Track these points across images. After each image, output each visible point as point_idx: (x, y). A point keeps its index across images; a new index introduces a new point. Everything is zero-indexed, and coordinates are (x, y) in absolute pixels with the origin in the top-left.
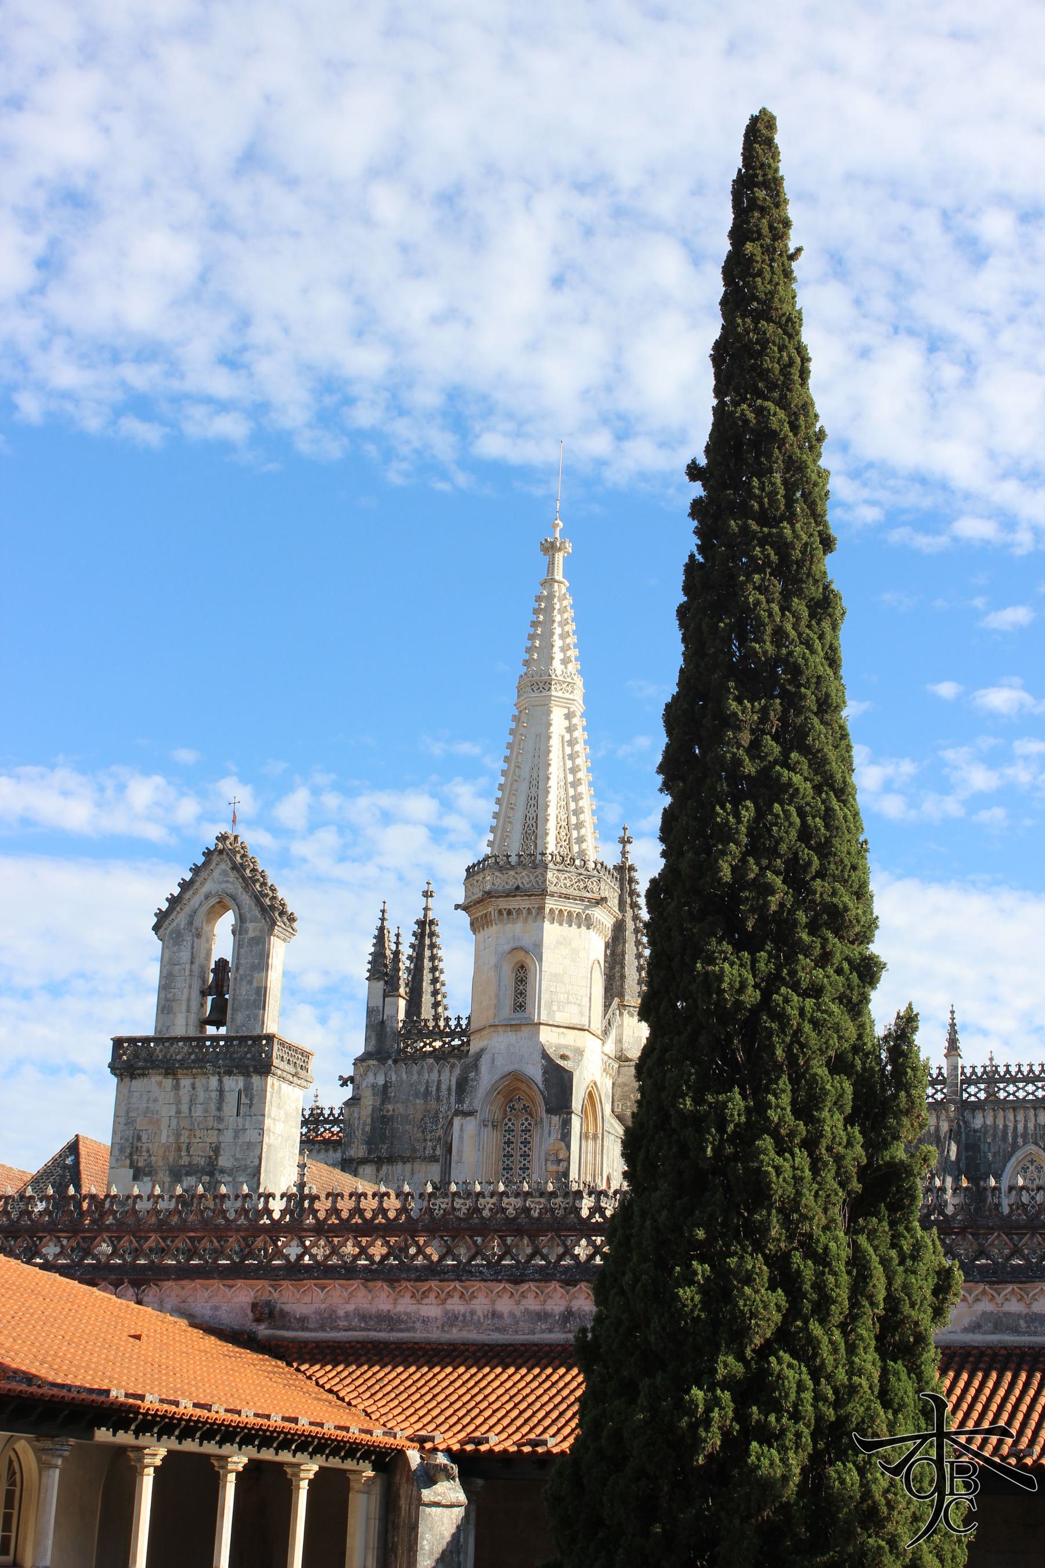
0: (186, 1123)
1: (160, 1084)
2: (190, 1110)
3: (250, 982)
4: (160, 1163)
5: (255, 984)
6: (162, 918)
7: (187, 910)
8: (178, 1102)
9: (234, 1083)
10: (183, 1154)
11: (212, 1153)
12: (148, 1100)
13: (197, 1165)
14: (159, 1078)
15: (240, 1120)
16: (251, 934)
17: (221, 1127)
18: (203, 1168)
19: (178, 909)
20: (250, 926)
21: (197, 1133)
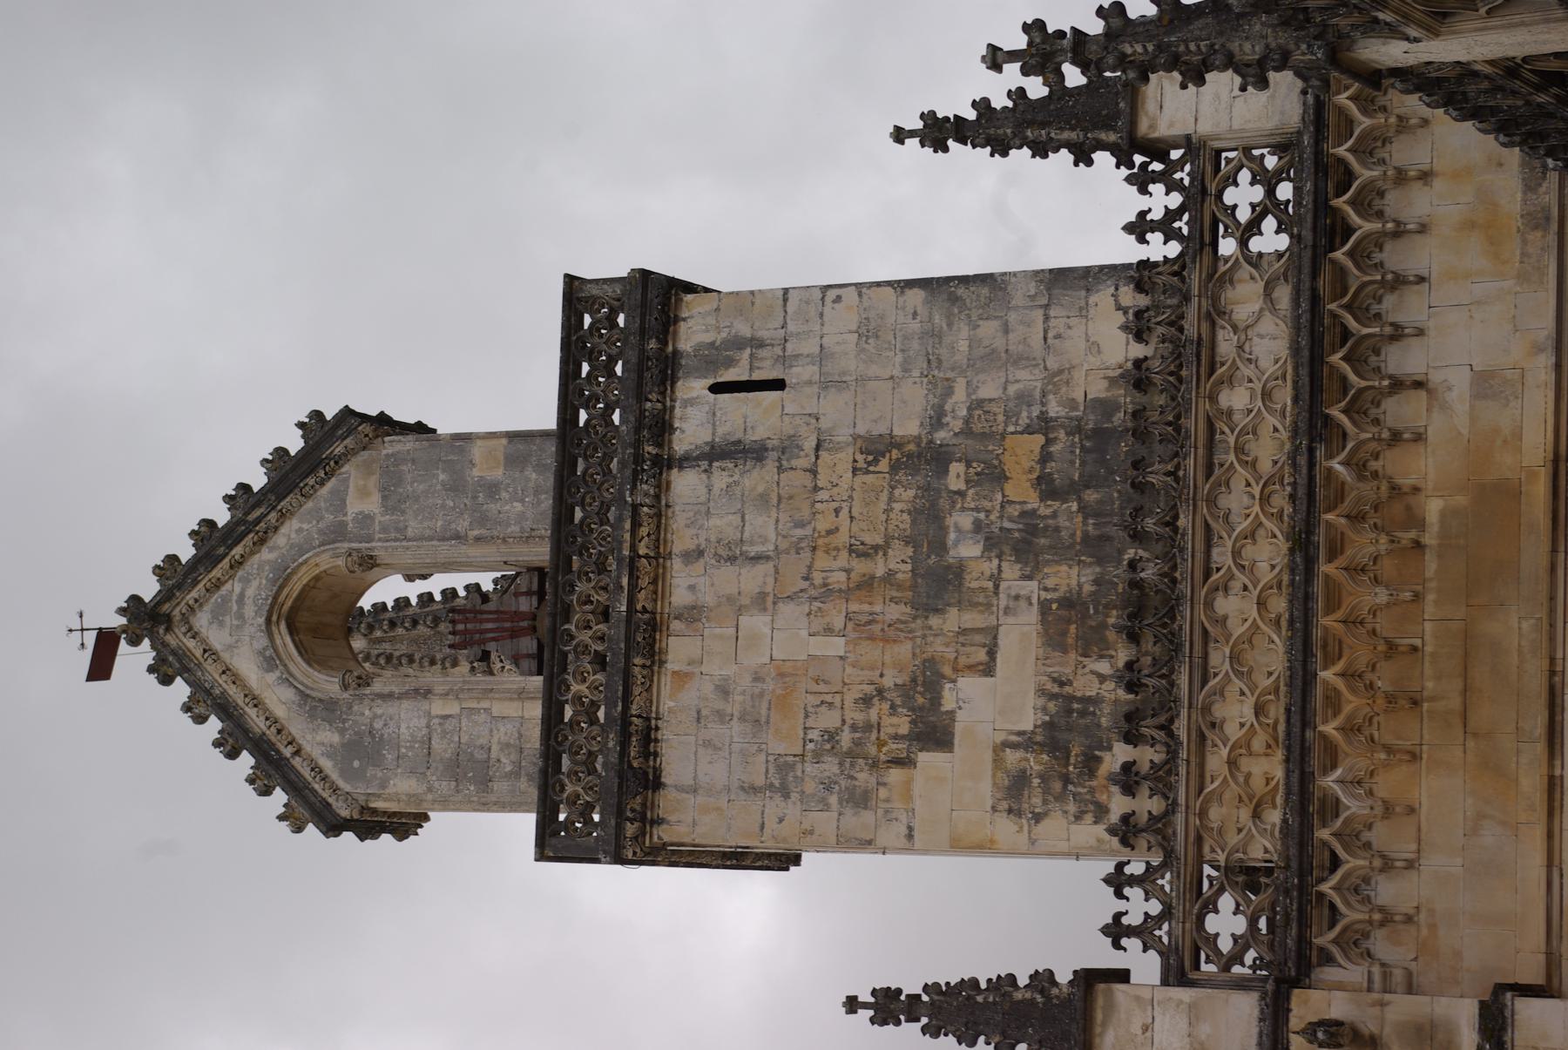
0: (793, 567)
1: (682, 677)
2: (758, 558)
3: (492, 489)
4: (904, 650)
5: (498, 474)
6: (315, 810)
7: (297, 728)
8: (736, 606)
9: (697, 416)
10: (880, 571)
11: (884, 465)
12: (722, 717)
13: (915, 513)
14: (666, 683)
15: (796, 374)
16: (373, 505)
17: (809, 444)
18: (926, 488)
19: (287, 752)
20: (354, 506)
21: (823, 524)
